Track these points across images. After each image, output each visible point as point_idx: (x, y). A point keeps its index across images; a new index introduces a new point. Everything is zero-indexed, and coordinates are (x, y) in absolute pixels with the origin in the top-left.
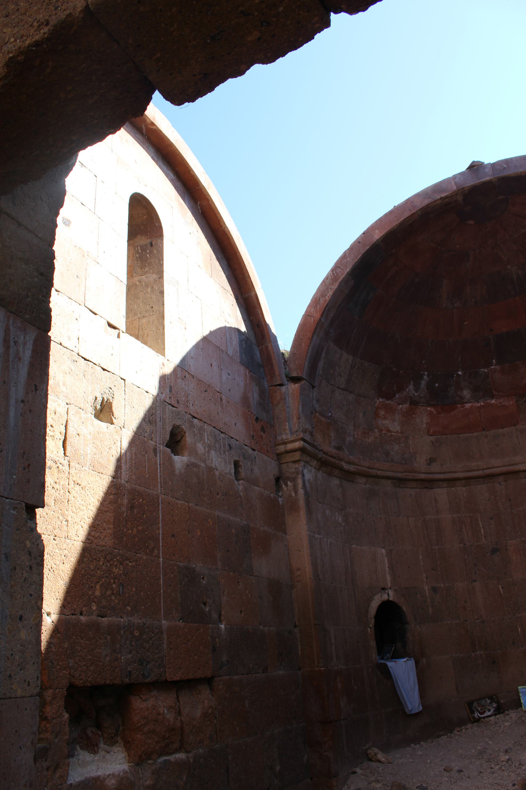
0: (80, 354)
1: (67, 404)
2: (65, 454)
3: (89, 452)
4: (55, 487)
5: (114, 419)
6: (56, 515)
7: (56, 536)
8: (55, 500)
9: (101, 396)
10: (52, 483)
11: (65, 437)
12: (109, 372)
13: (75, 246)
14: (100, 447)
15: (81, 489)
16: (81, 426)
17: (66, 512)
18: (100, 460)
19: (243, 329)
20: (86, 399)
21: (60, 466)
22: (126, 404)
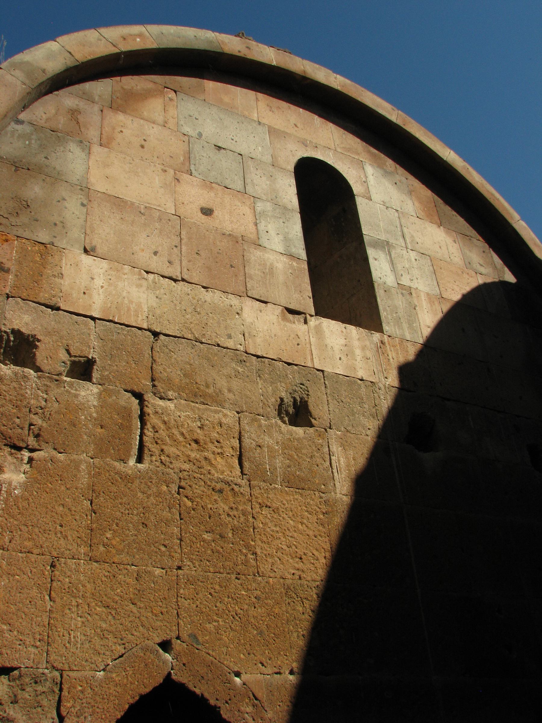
0: (248, 352)
1: (238, 413)
2: (242, 472)
3: (278, 465)
4: (231, 513)
5: (313, 420)
6: (237, 547)
7: (239, 574)
8: (233, 529)
9: (289, 396)
10: (226, 508)
11: (240, 452)
12: (296, 365)
13: (224, 234)
14: (295, 457)
15: (272, 512)
16: (262, 436)
17: (253, 543)
18: (298, 473)
19: (510, 278)
20: (266, 402)
21: (236, 488)
22: (329, 399)
